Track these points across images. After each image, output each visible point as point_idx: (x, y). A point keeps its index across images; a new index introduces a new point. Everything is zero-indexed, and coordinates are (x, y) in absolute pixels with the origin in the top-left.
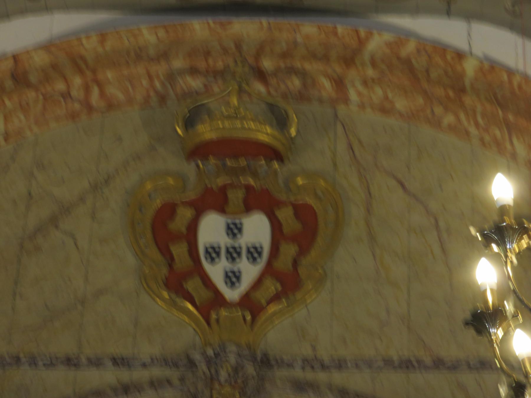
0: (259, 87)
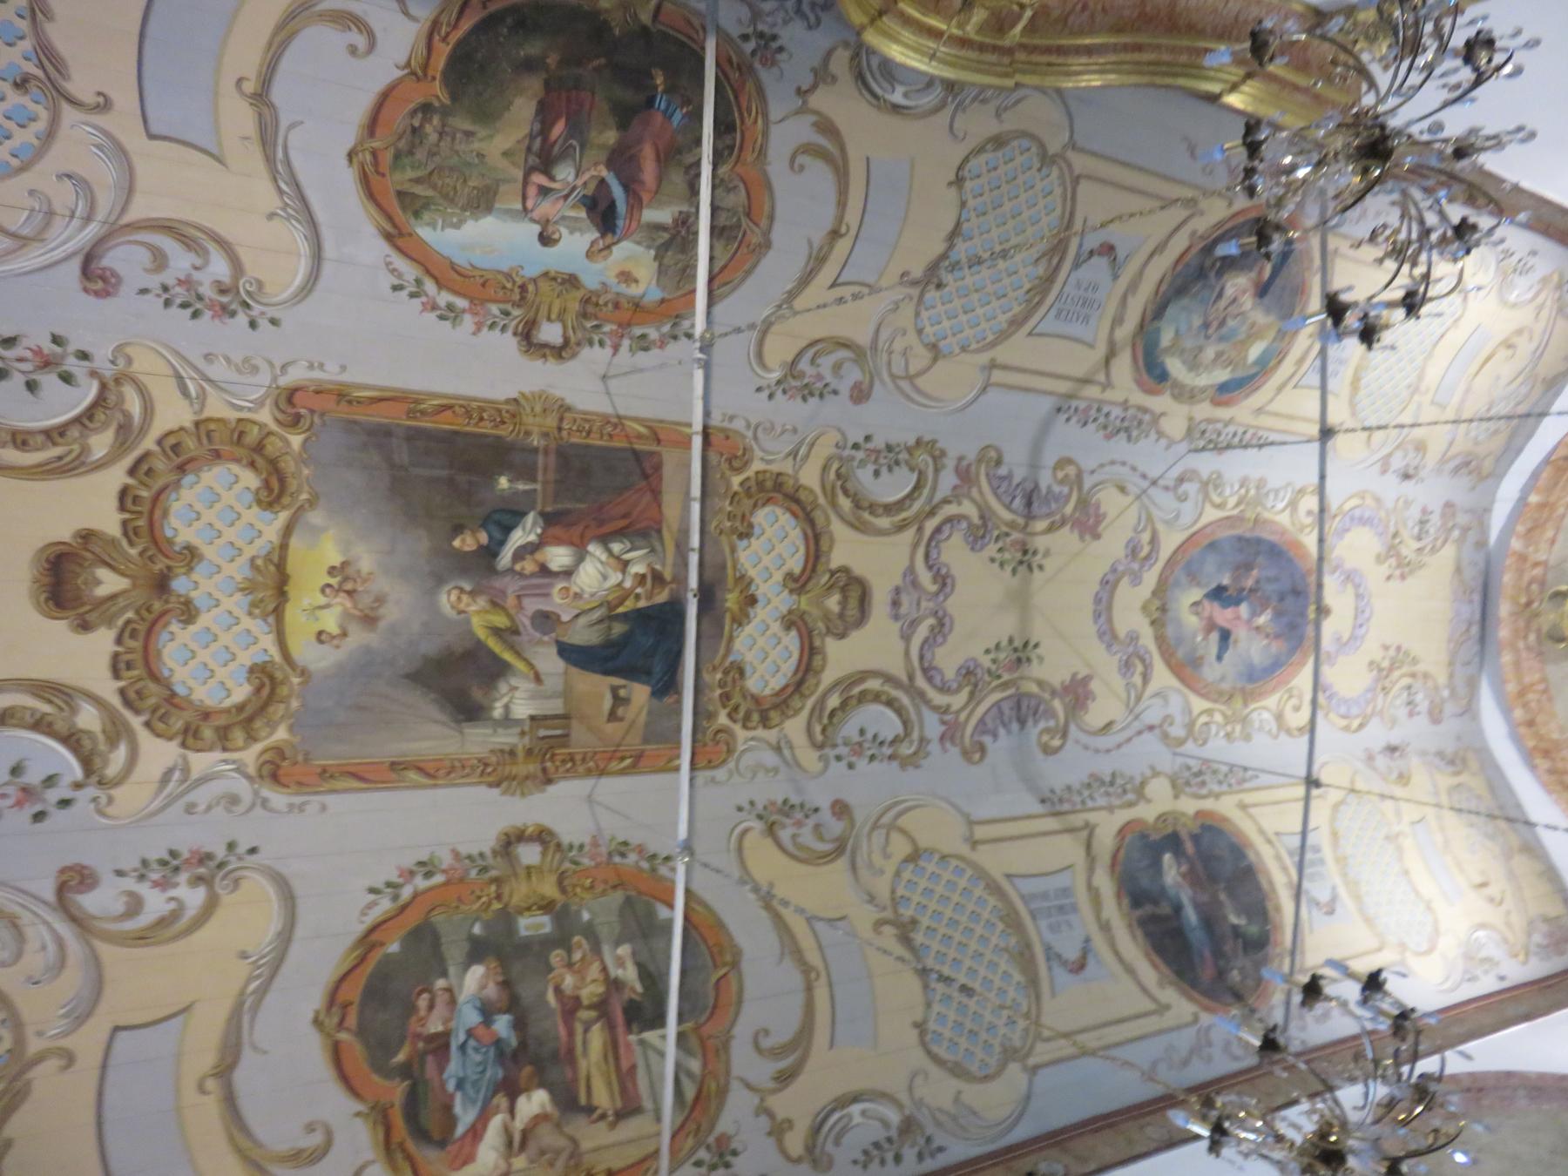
0: (1535, 605)
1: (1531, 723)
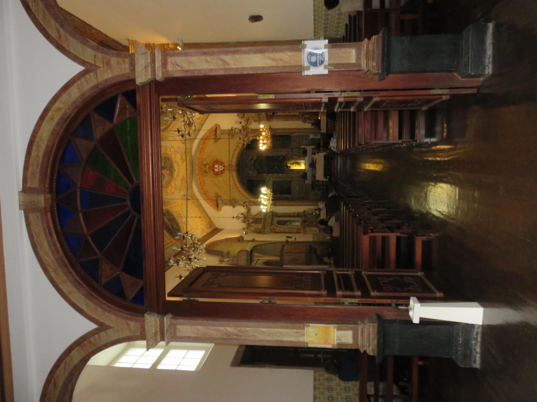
1: (202, 189)
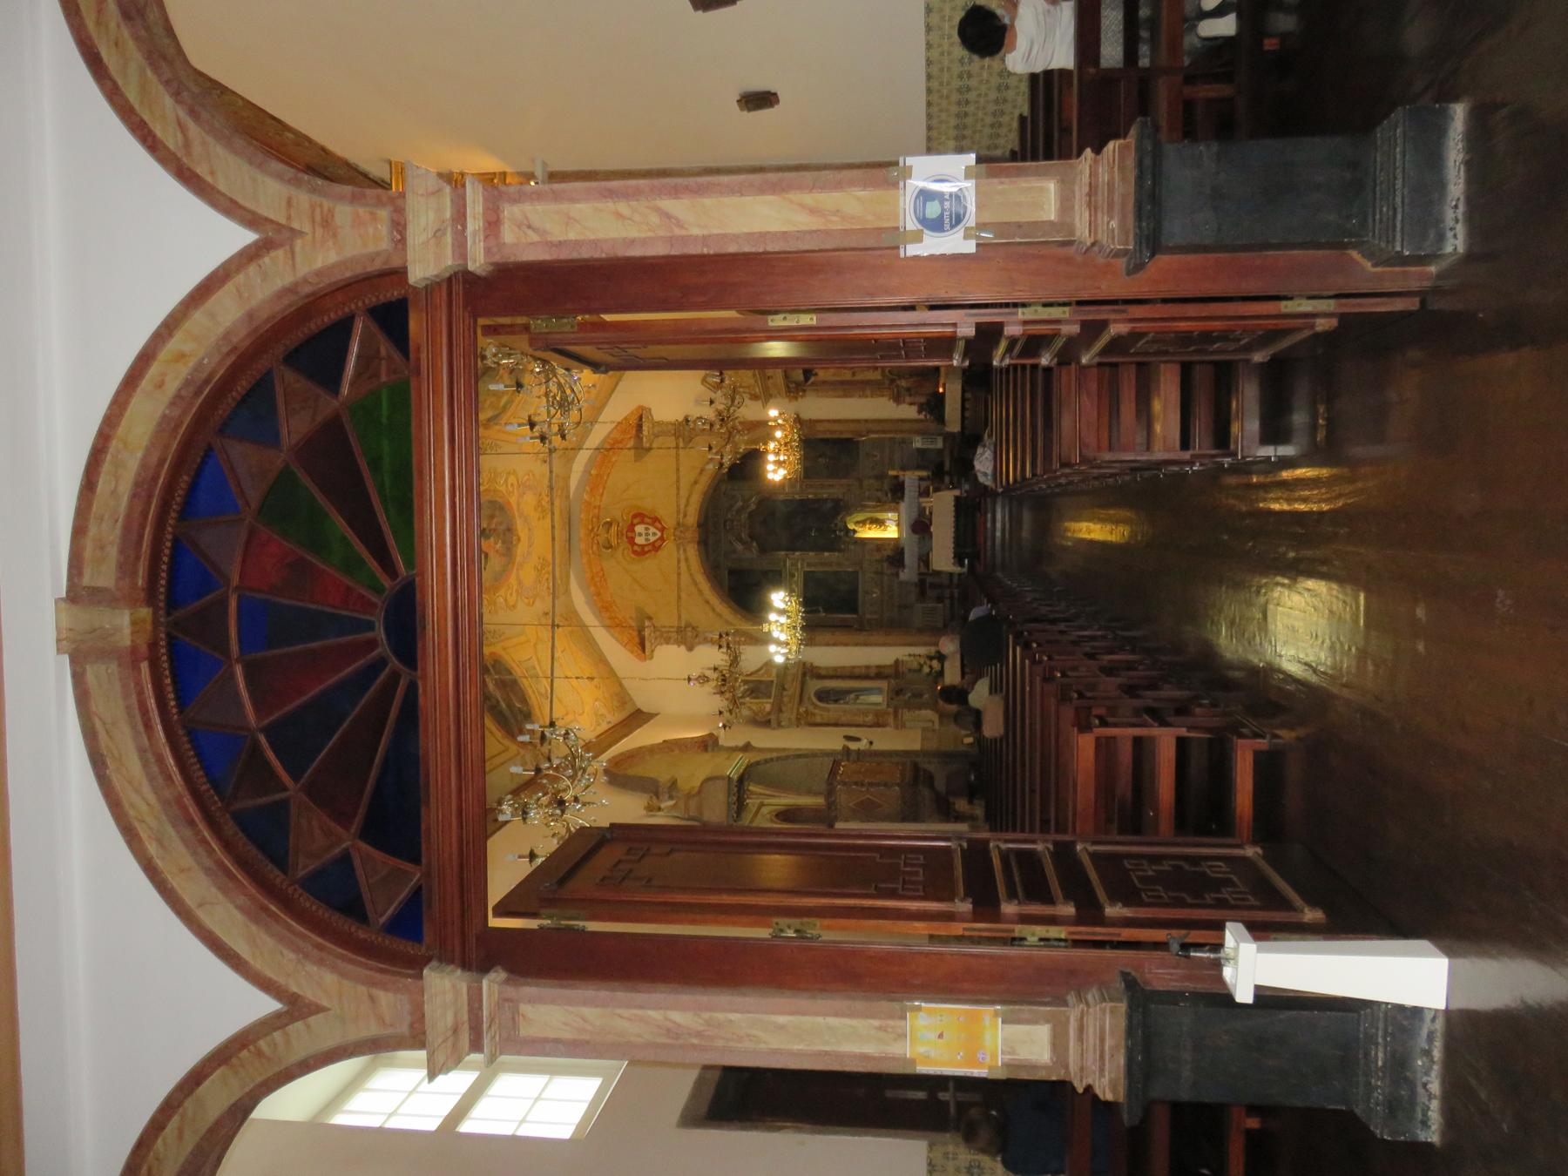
1: (598, 594)
